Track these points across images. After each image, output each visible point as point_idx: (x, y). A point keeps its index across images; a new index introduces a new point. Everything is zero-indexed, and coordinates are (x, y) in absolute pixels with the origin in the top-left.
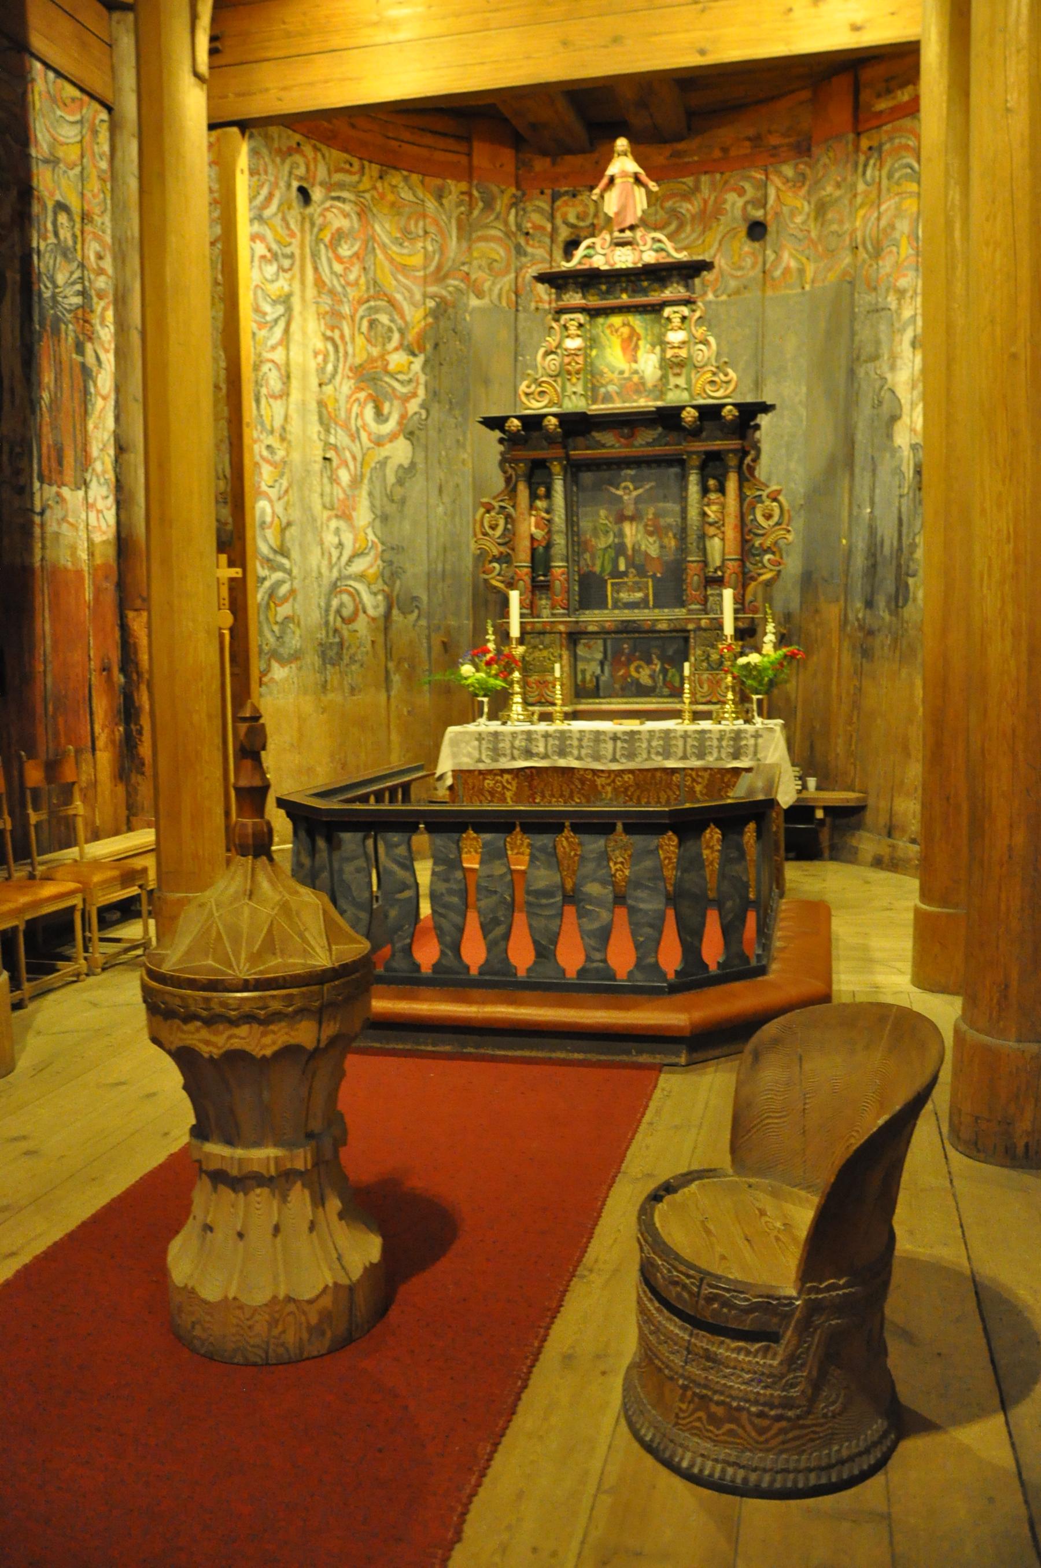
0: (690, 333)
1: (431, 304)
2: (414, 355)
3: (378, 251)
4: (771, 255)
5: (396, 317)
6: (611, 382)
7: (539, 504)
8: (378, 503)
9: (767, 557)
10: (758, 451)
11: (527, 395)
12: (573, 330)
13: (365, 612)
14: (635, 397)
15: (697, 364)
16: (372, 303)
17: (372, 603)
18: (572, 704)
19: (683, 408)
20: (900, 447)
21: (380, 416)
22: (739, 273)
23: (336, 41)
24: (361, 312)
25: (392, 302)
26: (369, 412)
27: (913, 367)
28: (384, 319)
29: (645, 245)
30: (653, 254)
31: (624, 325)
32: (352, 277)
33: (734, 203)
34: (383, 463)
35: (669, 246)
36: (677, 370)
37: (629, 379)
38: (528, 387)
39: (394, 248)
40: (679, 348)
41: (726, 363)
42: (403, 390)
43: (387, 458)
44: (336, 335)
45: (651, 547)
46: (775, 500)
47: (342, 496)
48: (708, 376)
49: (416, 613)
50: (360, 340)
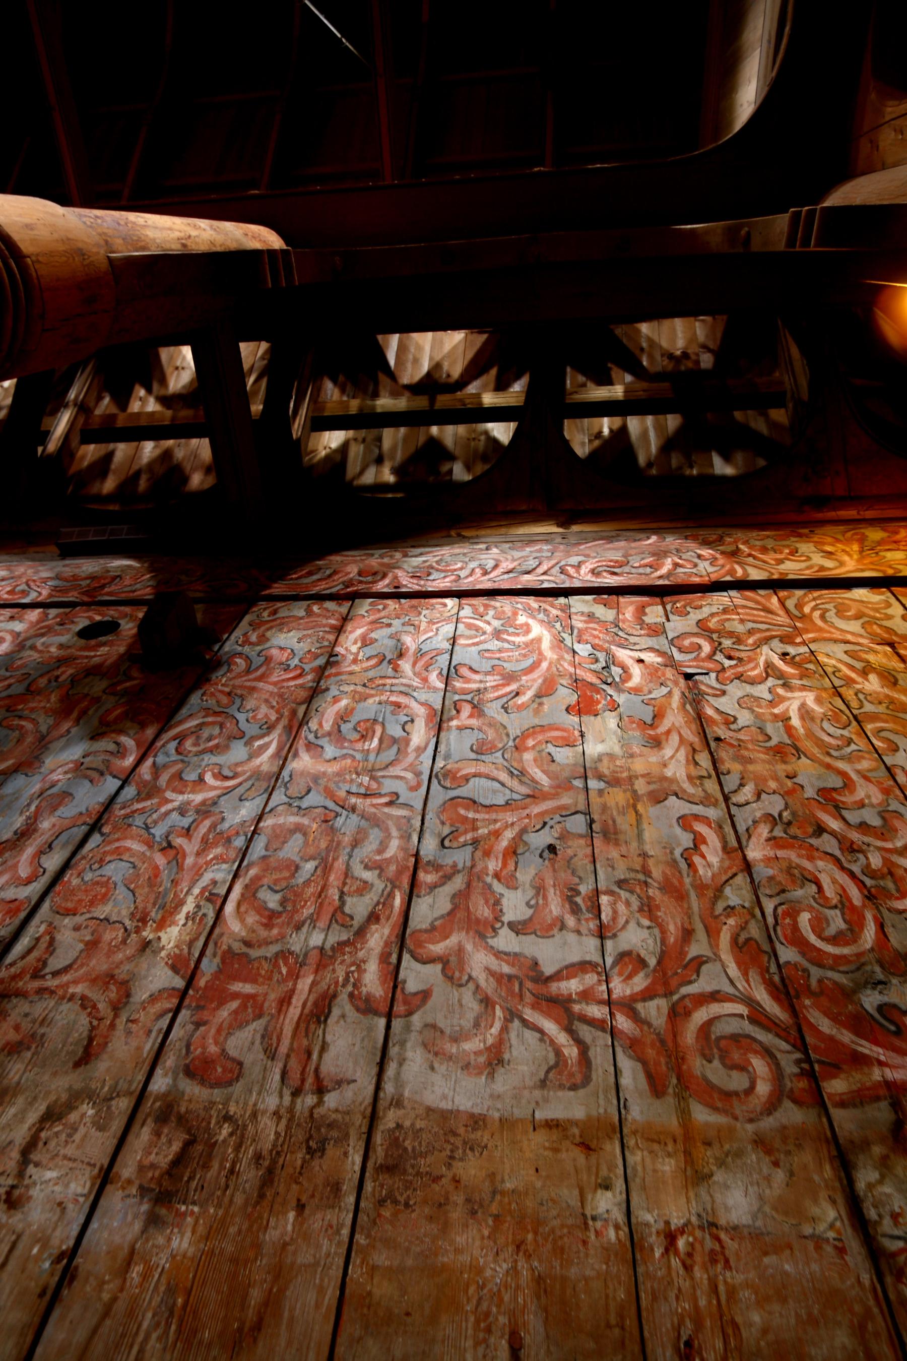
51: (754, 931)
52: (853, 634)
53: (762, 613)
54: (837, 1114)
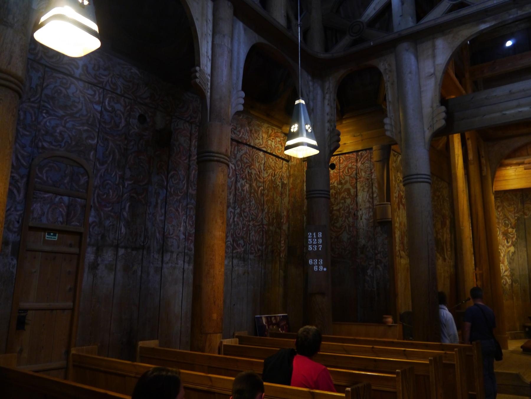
1: (516, 218)
3: (505, 208)
8: (508, 260)
13: (508, 283)
16: (505, 219)
17: (509, 281)
21: (508, 242)
23: (507, 178)
24: (503, 221)
25: (509, 219)
26: (506, 242)
28: (507, 222)
32: (501, 214)
34: (509, 252)
39: (508, 207)
43: (510, 251)
44: (499, 227)
47: (502, 259)
49: (517, 284)
50: (503, 227)
51: (233, 232)
52: (257, 168)
53: (249, 157)
54: (234, 255)
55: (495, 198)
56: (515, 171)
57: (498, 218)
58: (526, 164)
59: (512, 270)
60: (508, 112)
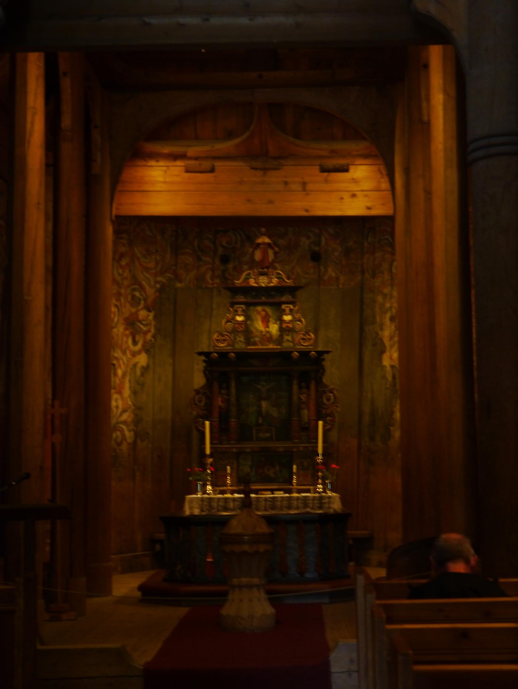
0: (293, 317)
1: (158, 286)
2: (150, 311)
4: (322, 269)
5: (143, 293)
6: (256, 336)
7: (223, 391)
9: (329, 418)
10: (324, 370)
11: (217, 340)
12: (240, 313)
13: (126, 440)
14: (267, 343)
15: (297, 330)
16: (133, 287)
17: (129, 435)
18: (237, 486)
19: (292, 352)
20: (385, 366)
21: (135, 343)
22: (307, 276)
26: (130, 341)
27: (390, 330)
28: (137, 294)
29: (273, 275)
30: (276, 279)
31: (264, 310)
33: (305, 242)
34: (135, 365)
35: (284, 276)
36: (288, 333)
37: (265, 335)
38: (218, 337)
40: (289, 323)
41: (309, 330)
42: (145, 329)
45: (274, 412)
46: (332, 393)
48: (301, 336)
50: (128, 305)
55: (117, 233)
56: (165, 172)
57: (118, 284)
58: (190, 158)
59: (138, 409)
60: (154, 21)
